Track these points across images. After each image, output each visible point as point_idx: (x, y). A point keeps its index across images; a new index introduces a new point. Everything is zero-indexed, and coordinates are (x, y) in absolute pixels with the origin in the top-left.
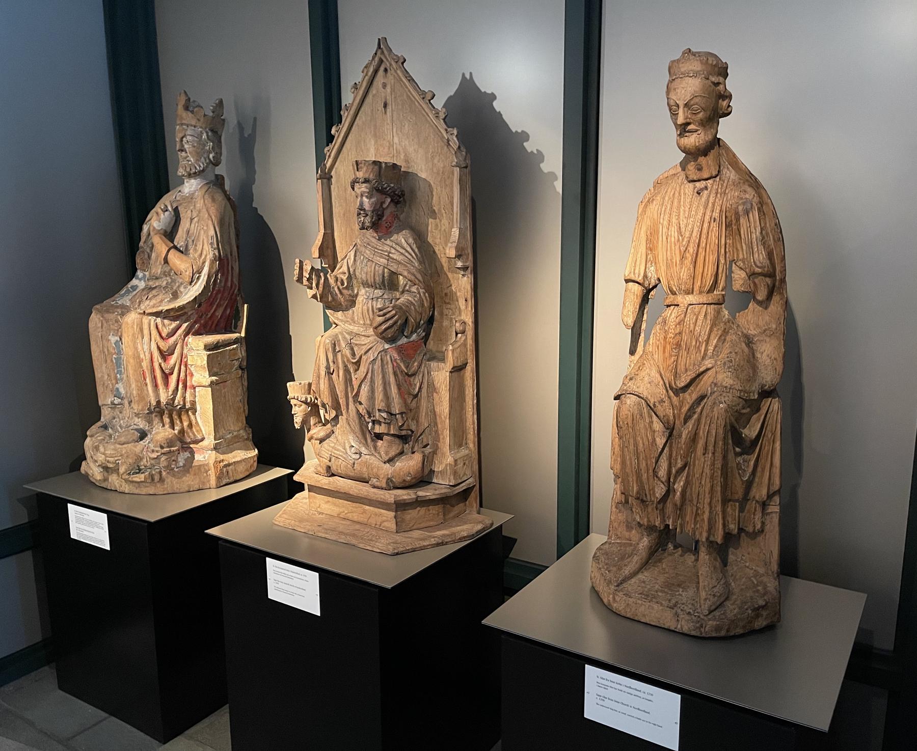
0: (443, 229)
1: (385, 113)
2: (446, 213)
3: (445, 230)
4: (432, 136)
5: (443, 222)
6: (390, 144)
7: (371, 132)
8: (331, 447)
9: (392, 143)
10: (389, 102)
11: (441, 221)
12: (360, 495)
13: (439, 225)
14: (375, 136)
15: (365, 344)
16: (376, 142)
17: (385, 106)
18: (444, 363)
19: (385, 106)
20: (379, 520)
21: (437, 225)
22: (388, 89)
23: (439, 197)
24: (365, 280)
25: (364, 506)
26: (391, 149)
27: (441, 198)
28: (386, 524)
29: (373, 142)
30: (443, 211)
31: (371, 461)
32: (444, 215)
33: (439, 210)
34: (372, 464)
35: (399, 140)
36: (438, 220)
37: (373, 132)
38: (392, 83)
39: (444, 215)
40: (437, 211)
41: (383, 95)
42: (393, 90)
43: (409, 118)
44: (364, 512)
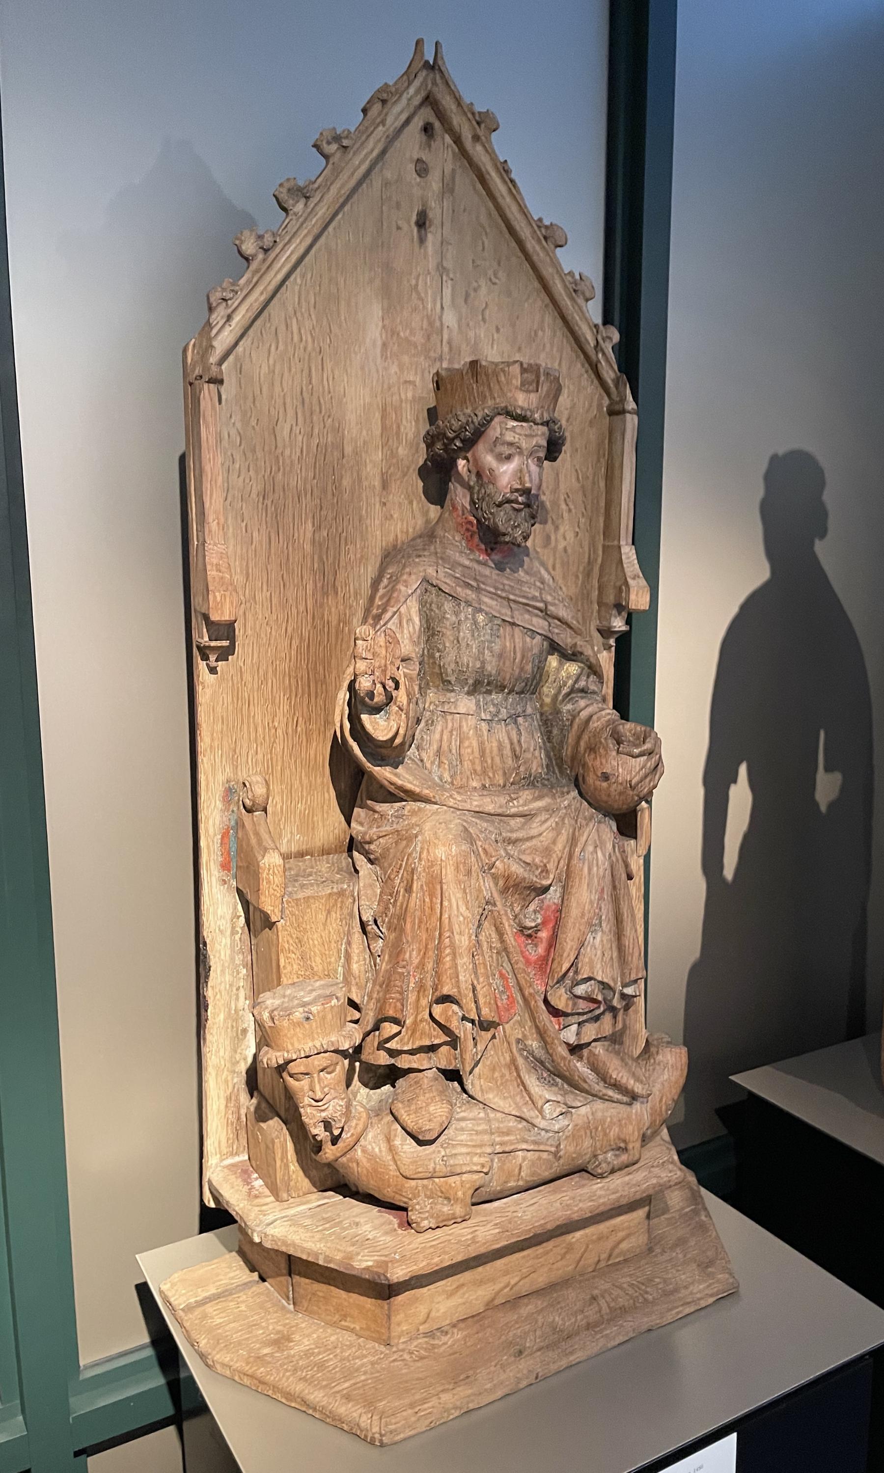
0: (561, 547)
1: (422, 240)
2: (570, 510)
3: (565, 550)
4: (548, 332)
5: (562, 530)
6: (431, 324)
7: (371, 281)
8: (484, 1132)
9: (438, 324)
10: (434, 214)
11: (557, 528)
12: (602, 1209)
13: (553, 538)
14: (386, 292)
15: (540, 834)
16: (388, 311)
17: (422, 223)
18: (636, 838)
19: (422, 223)
20: (609, 1244)
21: (548, 538)
22: (434, 182)
23: (557, 475)
24: (494, 672)
25: (571, 1235)
26: (435, 338)
27: (562, 478)
28: (624, 1246)
29: (377, 310)
30: (564, 506)
31: (599, 1115)
32: (566, 515)
33: (555, 503)
34: (603, 1121)
35: (459, 321)
36: (549, 526)
37: (377, 282)
38: (448, 171)
39: (566, 515)
40: (548, 504)
41: (417, 192)
42: (448, 188)
43: (490, 273)
44: (570, 1248)
